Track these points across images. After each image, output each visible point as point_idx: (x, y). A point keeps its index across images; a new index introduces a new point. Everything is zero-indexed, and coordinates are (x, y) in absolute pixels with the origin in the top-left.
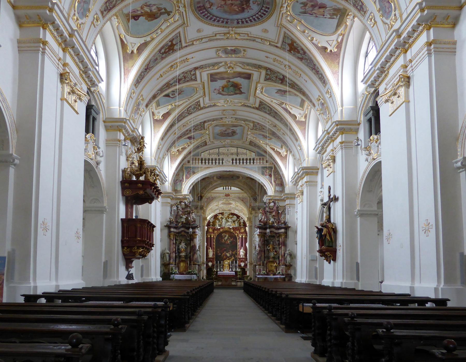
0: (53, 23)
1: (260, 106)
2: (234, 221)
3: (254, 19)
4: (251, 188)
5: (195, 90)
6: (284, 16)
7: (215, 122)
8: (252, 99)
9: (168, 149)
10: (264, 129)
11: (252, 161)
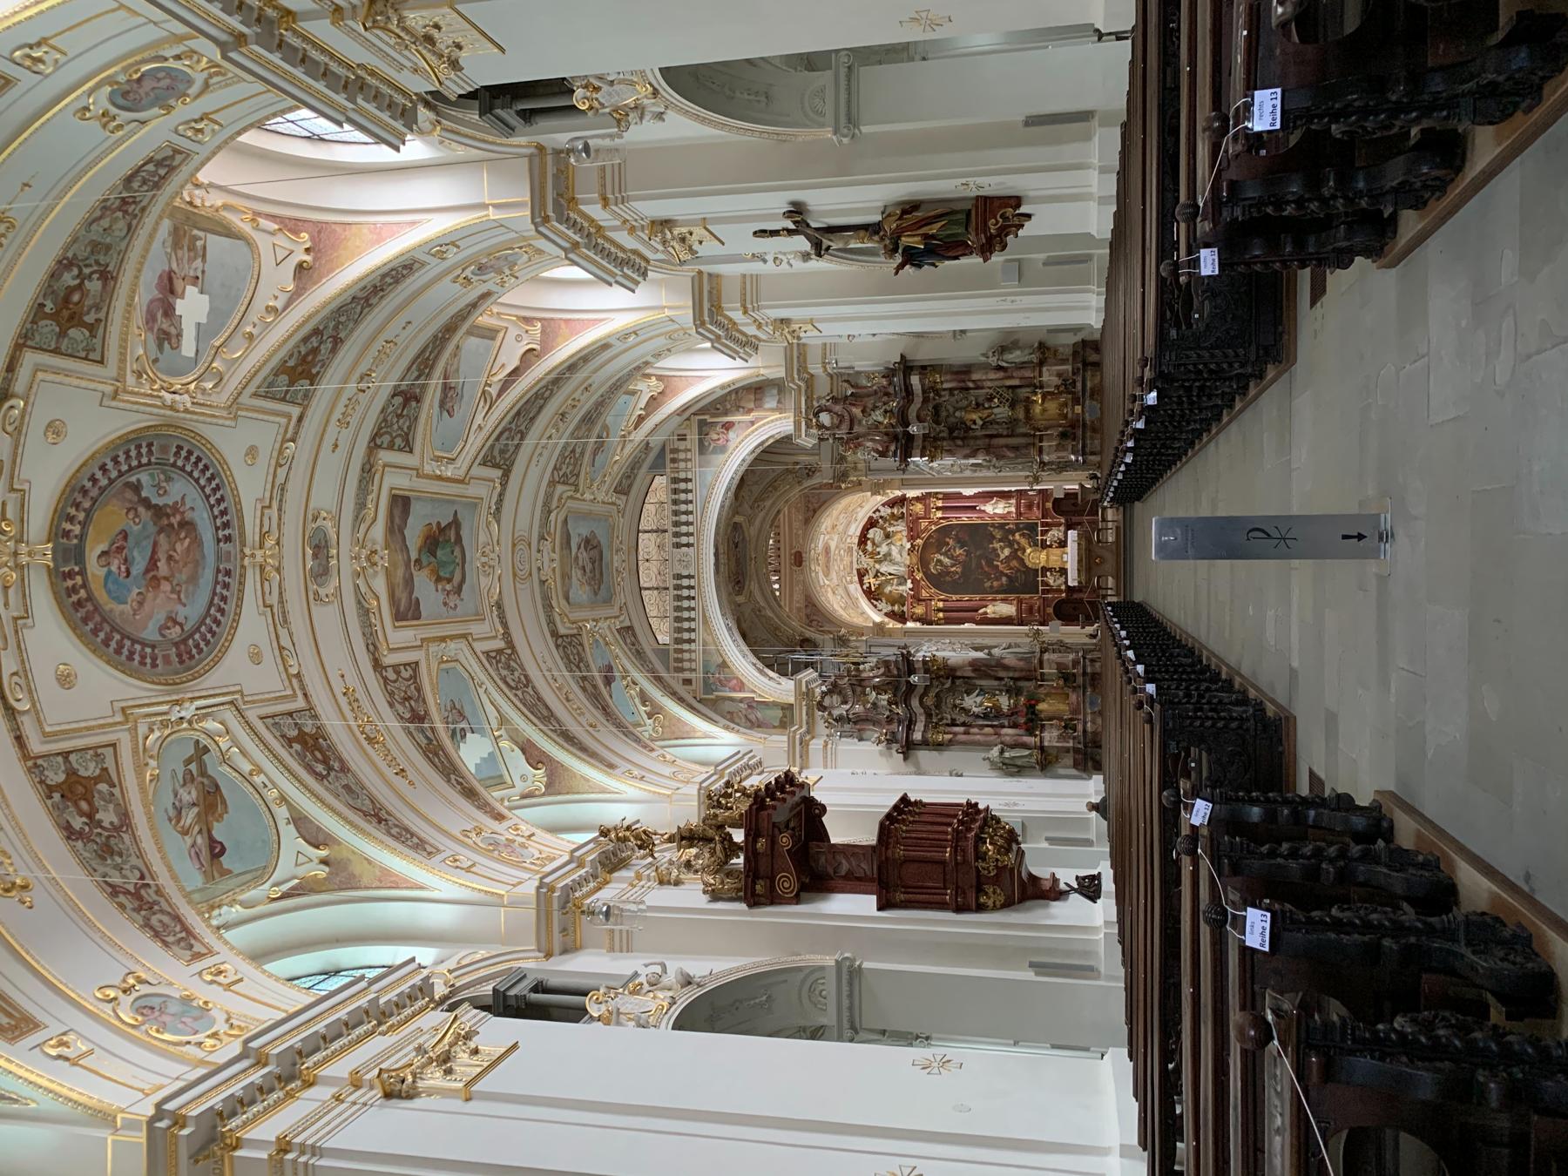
0: (221, 1115)
1: (496, 466)
2: (887, 536)
3: (215, 490)
4: (773, 486)
5: (448, 666)
6: (200, 398)
7: (554, 603)
8: (474, 490)
9: (645, 747)
10: (573, 451)
11: (682, 486)
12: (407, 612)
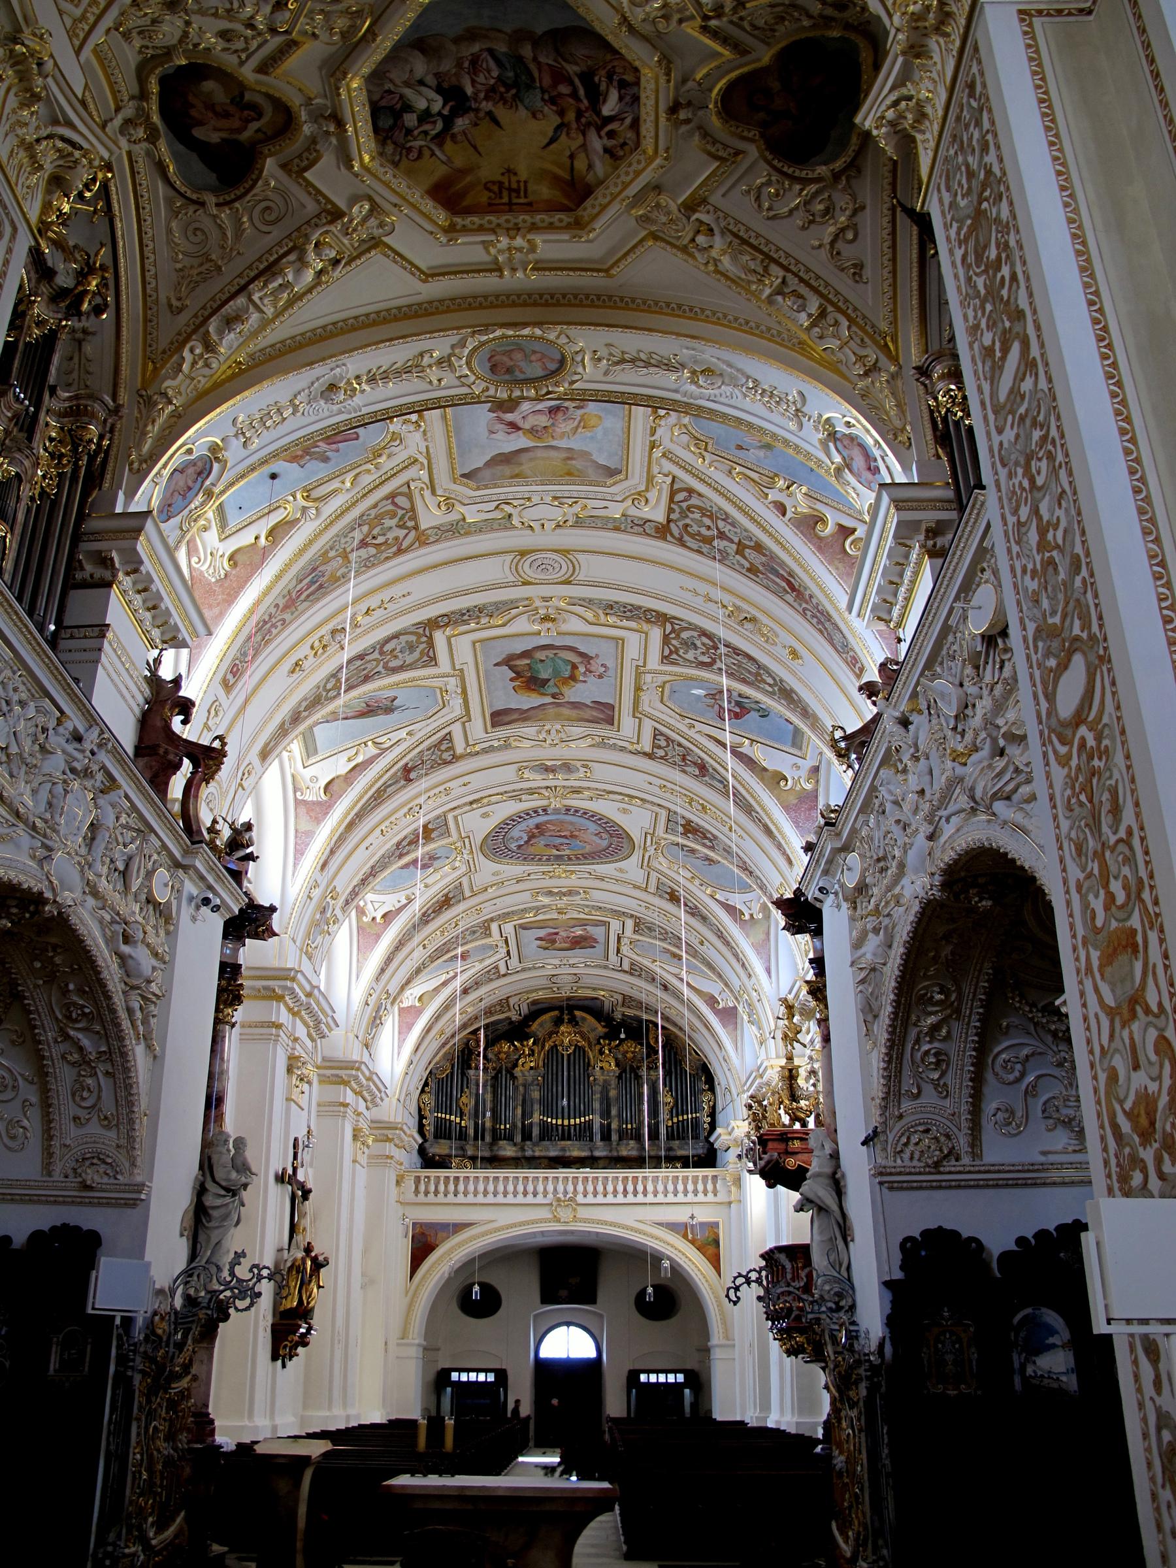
10: (363, 544)
12: (606, 714)
